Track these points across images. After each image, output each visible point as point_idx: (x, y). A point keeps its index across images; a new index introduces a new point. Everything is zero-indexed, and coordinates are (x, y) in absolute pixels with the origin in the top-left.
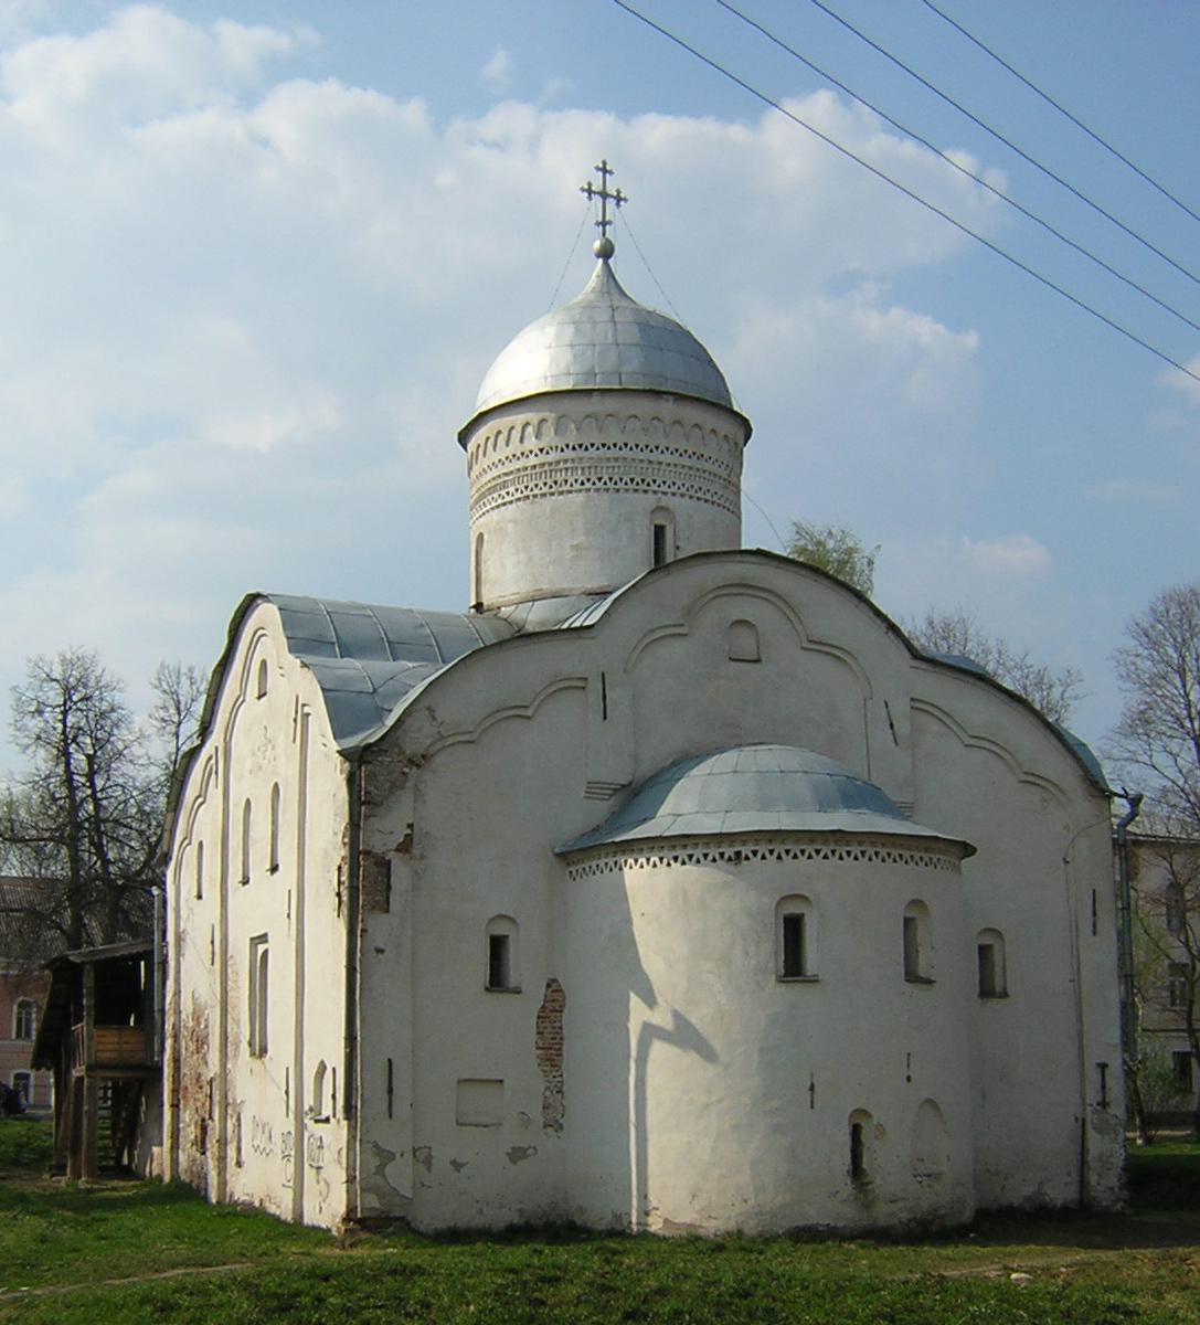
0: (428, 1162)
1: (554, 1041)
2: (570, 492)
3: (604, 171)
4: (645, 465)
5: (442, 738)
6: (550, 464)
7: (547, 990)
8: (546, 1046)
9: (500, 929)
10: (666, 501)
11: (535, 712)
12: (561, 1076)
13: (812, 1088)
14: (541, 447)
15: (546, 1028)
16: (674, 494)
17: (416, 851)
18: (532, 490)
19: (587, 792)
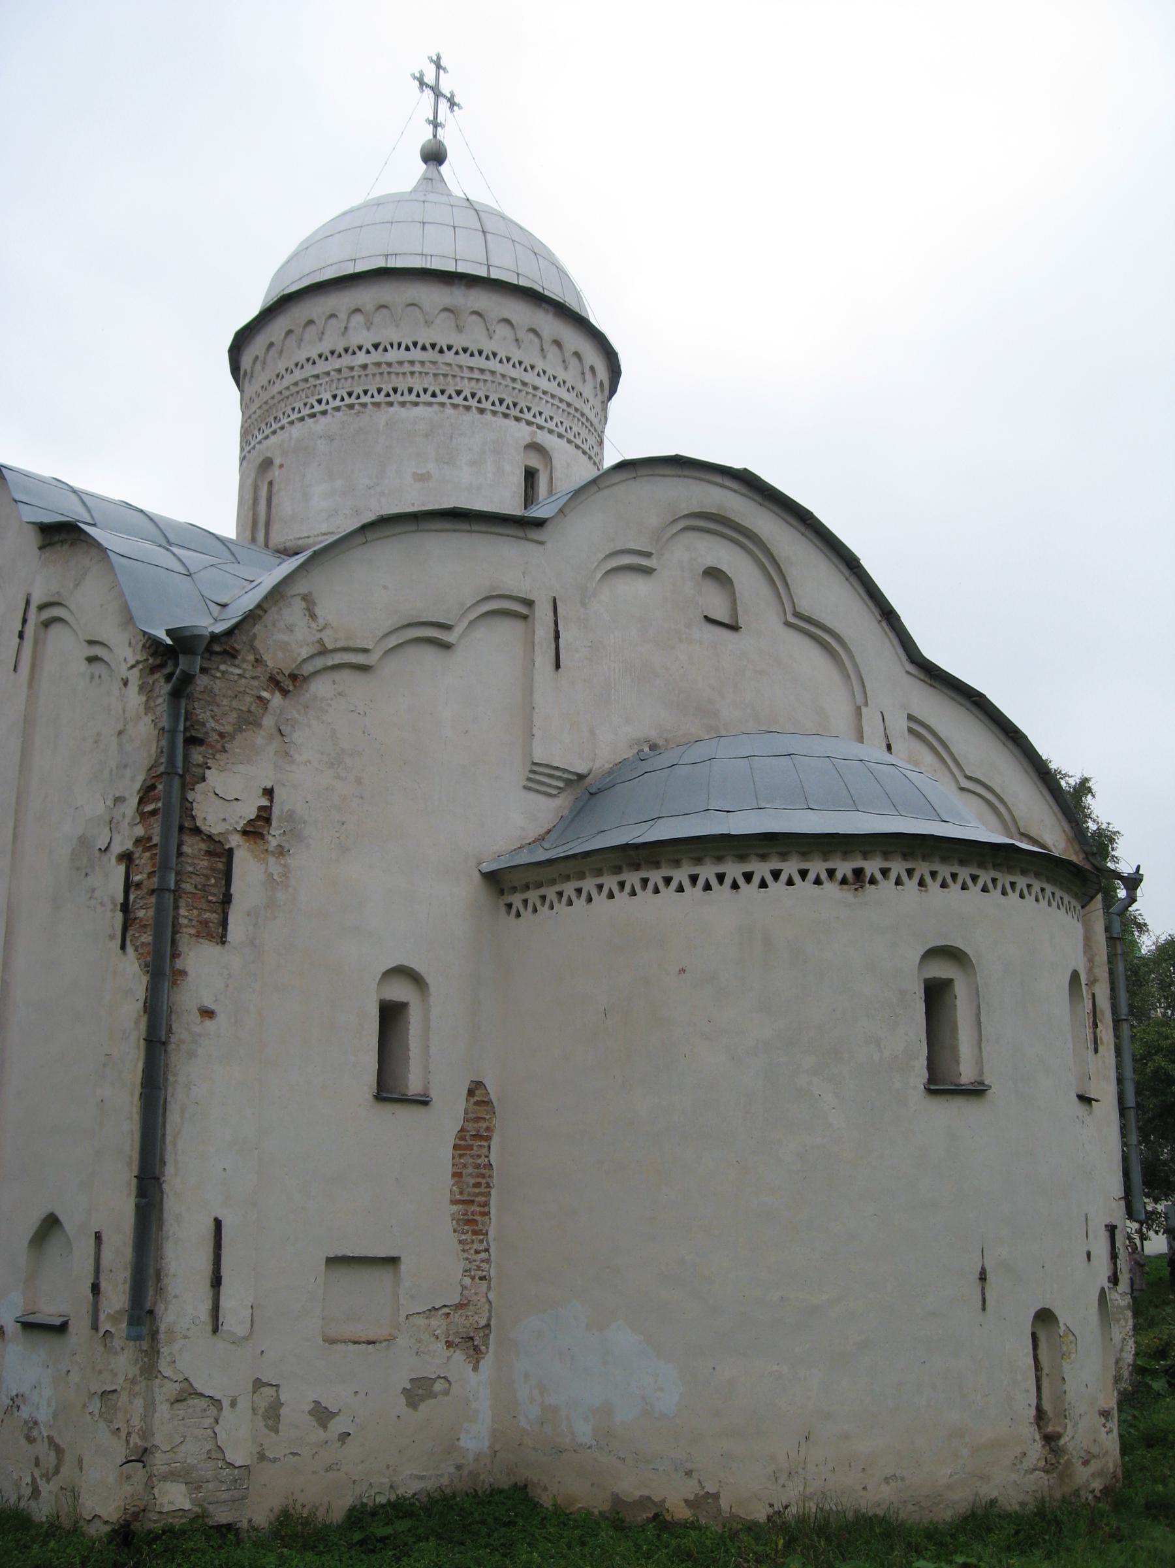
0: (273, 1415)
1: (477, 1190)
2: (416, 404)
3: (439, 67)
4: (518, 386)
5: (324, 652)
6: (389, 365)
7: (467, 1101)
8: (465, 1197)
9: (399, 992)
10: (543, 438)
11: (461, 636)
12: (487, 1250)
13: (983, 1277)
14: (377, 341)
15: (465, 1166)
18: (358, 397)
19: (529, 779)
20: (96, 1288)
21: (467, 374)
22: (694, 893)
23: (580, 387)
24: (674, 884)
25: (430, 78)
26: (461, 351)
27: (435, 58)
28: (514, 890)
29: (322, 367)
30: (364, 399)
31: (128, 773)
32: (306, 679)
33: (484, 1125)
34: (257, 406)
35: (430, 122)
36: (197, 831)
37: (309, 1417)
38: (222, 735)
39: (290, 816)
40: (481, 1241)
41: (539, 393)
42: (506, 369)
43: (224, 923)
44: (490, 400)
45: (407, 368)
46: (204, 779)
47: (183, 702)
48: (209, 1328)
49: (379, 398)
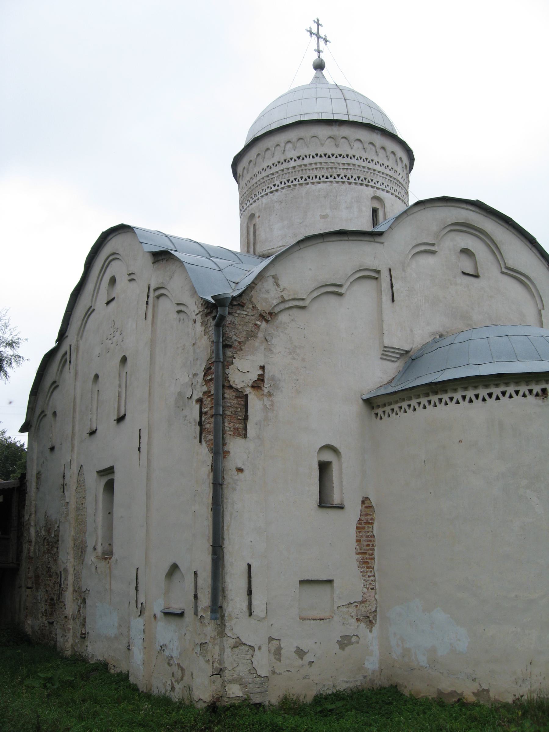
0: (278, 652)
1: (368, 548)
2: (319, 183)
3: (318, 24)
4: (366, 170)
5: (284, 301)
6: (305, 165)
7: (362, 506)
8: (363, 551)
9: (327, 457)
10: (379, 193)
11: (347, 290)
12: (374, 576)
15: (362, 537)
16: (383, 190)
17: (266, 389)
18: (292, 182)
19: (383, 354)
20: (196, 597)
21: (342, 166)
22: (464, 404)
23: (395, 168)
24: (455, 400)
25: (314, 30)
26: (338, 156)
27: (316, 21)
28: (378, 407)
29: (274, 169)
30: (295, 183)
31: (199, 362)
32: (276, 314)
33: (370, 517)
34: (246, 190)
35: (316, 51)
36: (231, 387)
37: (294, 654)
38: (239, 343)
39: (273, 378)
40: (371, 571)
41: (376, 172)
42: (360, 162)
43: (245, 428)
44: (354, 178)
45: (314, 166)
46: (233, 363)
47: (221, 329)
48: (248, 614)
49: (302, 181)
